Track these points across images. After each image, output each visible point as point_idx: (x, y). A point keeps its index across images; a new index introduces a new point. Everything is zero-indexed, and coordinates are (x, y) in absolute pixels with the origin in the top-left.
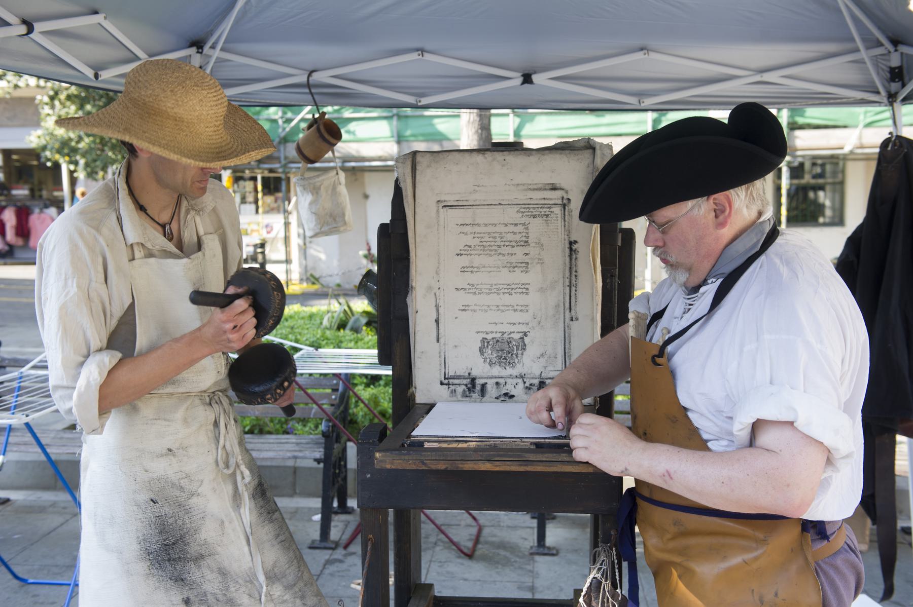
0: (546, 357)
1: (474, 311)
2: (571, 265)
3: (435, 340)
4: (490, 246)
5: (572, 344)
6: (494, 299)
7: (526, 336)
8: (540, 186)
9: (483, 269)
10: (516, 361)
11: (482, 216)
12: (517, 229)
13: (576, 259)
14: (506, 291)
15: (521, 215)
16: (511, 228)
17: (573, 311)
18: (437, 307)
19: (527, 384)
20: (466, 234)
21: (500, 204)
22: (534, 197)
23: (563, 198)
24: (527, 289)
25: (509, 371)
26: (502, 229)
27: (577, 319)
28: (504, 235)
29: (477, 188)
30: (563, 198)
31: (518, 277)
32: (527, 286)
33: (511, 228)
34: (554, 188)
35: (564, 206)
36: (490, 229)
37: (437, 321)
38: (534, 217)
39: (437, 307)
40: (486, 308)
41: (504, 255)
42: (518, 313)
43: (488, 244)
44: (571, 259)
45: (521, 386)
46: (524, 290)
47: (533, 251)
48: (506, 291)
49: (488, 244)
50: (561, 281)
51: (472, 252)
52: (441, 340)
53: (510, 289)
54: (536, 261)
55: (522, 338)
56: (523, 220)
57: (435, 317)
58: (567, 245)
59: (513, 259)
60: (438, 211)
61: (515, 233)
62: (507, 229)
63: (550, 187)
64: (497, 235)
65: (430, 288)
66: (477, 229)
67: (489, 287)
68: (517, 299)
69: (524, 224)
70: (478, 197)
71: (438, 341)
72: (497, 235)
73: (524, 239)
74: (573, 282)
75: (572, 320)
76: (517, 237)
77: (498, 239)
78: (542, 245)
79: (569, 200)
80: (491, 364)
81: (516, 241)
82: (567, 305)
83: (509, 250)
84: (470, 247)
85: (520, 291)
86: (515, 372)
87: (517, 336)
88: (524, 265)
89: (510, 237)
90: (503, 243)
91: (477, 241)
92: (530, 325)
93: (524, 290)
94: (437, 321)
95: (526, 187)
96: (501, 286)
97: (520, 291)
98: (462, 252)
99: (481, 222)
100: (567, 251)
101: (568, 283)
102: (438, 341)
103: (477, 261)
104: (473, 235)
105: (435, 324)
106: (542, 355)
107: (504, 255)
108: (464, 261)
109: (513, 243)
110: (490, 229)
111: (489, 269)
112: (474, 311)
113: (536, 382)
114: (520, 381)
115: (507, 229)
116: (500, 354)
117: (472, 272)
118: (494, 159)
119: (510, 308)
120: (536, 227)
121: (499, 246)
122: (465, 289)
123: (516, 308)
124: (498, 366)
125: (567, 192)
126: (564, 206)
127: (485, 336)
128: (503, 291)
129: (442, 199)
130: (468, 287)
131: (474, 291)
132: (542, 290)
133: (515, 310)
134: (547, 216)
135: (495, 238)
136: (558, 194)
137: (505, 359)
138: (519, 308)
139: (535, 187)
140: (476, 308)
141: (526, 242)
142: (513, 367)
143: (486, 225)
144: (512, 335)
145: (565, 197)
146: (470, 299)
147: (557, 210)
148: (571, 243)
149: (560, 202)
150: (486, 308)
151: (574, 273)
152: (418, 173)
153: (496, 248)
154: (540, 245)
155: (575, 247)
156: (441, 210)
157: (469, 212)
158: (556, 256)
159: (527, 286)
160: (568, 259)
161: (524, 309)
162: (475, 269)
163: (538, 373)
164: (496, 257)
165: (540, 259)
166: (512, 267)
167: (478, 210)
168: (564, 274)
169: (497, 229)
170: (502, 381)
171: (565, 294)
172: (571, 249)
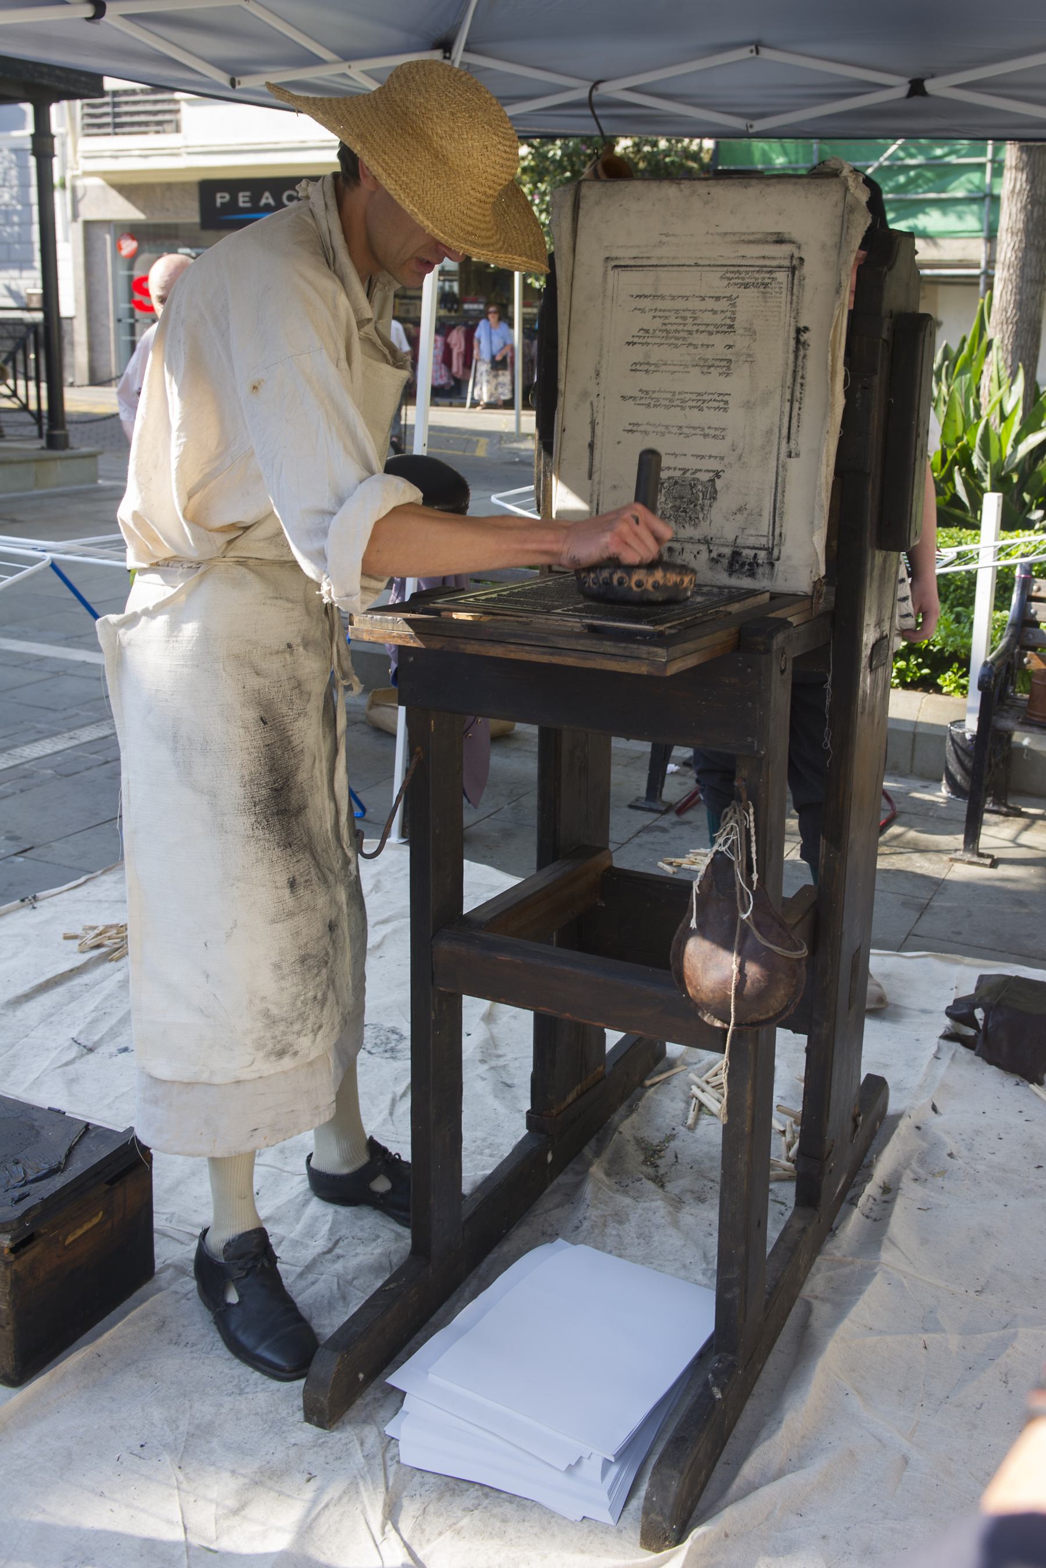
1: (646, 433)
2: (796, 366)
3: (586, 476)
4: (676, 331)
5: (786, 493)
7: (719, 477)
8: (758, 236)
9: (664, 368)
10: (701, 516)
11: (670, 282)
13: (805, 356)
14: (694, 404)
15: (726, 282)
16: (710, 304)
17: (792, 442)
18: (593, 423)
19: (714, 555)
20: (643, 311)
21: (697, 265)
22: (748, 254)
23: (792, 256)
24: (726, 402)
25: (688, 531)
26: (697, 304)
27: (797, 455)
28: (698, 314)
29: (664, 239)
30: (792, 256)
32: (726, 398)
33: (710, 304)
35: (793, 269)
36: (680, 304)
37: (591, 446)
38: (746, 286)
39: (593, 423)
40: (663, 429)
41: (695, 346)
42: (710, 440)
43: (674, 327)
44: (796, 357)
45: (704, 556)
46: (721, 405)
47: (740, 342)
49: (674, 327)
50: (779, 391)
51: (649, 340)
52: (596, 477)
53: (700, 401)
54: (743, 358)
55: (712, 481)
56: (729, 291)
57: (589, 439)
58: (793, 335)
59: (709, 354)
60: (605, 274)
61: (715, 312)
62: (703, 305)
63: (775, 238)
64: (688, 314)
65: (585, 394)
66: (659, 304)
67: (669, 396)
68: (710, 418)
69: (730, 298)
71: (590, 477)
72: (688, 314)
73: (728, 322)
74: (797, 394)
75: (790, 456)
76: (718, 319)
77: (689, 321)
78: (755, 333)
79: (801, 259)
82: (785, 431)
83: (703, 338)
84: (647, 331)
85: (716, 404)
86: (696, 533)
87: (704, 477)
88: (724, 363)
89: (708, 318)
90: (695, 328)
91: (658, 323)
92: (726, 461)
93: (721, 405)
94: (591, 446)
96: (688, 396)
97: (716, 404)
98: (636, 340)
99: (666, 293)
100: (792, 343)
101: (788, 397)
102: (590, 477)
103: (657, 354)
104: (652, 313)
106: (740, 510)
107: (695, 346)
108: (637, 354)
109: (711, 328)
110: (680, 304)
111: (673, 368)
113: (727, 551)
114: (703, 548)
116: (678, 503)
119: (698, 431)
120: (748, 301)
121: (690, 332)
122: (635, 398)
123: (707, 431)
124: (673, 523)
125: (799, 247)
126: (793, 269)
128: (690, 403)
129: (614, 255)
130: (640, 394)
133: (705, 436)
134: (766, 285)
135: (684, 318)
136: (786, 249)
137: (685, 511)
138: (712, 432)
139: (752, 238)
140: (650, 429)
141: (731, 326)
142: (696, 526)
143: (673, 298)
144: (698, 475)
145: (796, 255)
147: (782, 277)
148: (799, 331)
149: (787, 263)
150: (663, 429)
151: (799, 380)
152: (581, 213)
153: (685, 335)
154: (751, 332)
155: (804, 337)
156: (610, 273)
157: (650, 275)
158: (775, 353)
159: (726, 398)
160: (791, 356)
162: (652, 368)
163: (731, 538)
164: (683, 350)
165: (749, 355)
166: (706, 366)
167: (663, 274)
168: (784, 381)
170: (677, 546)
171: (782, 413)
172: (798, 341)
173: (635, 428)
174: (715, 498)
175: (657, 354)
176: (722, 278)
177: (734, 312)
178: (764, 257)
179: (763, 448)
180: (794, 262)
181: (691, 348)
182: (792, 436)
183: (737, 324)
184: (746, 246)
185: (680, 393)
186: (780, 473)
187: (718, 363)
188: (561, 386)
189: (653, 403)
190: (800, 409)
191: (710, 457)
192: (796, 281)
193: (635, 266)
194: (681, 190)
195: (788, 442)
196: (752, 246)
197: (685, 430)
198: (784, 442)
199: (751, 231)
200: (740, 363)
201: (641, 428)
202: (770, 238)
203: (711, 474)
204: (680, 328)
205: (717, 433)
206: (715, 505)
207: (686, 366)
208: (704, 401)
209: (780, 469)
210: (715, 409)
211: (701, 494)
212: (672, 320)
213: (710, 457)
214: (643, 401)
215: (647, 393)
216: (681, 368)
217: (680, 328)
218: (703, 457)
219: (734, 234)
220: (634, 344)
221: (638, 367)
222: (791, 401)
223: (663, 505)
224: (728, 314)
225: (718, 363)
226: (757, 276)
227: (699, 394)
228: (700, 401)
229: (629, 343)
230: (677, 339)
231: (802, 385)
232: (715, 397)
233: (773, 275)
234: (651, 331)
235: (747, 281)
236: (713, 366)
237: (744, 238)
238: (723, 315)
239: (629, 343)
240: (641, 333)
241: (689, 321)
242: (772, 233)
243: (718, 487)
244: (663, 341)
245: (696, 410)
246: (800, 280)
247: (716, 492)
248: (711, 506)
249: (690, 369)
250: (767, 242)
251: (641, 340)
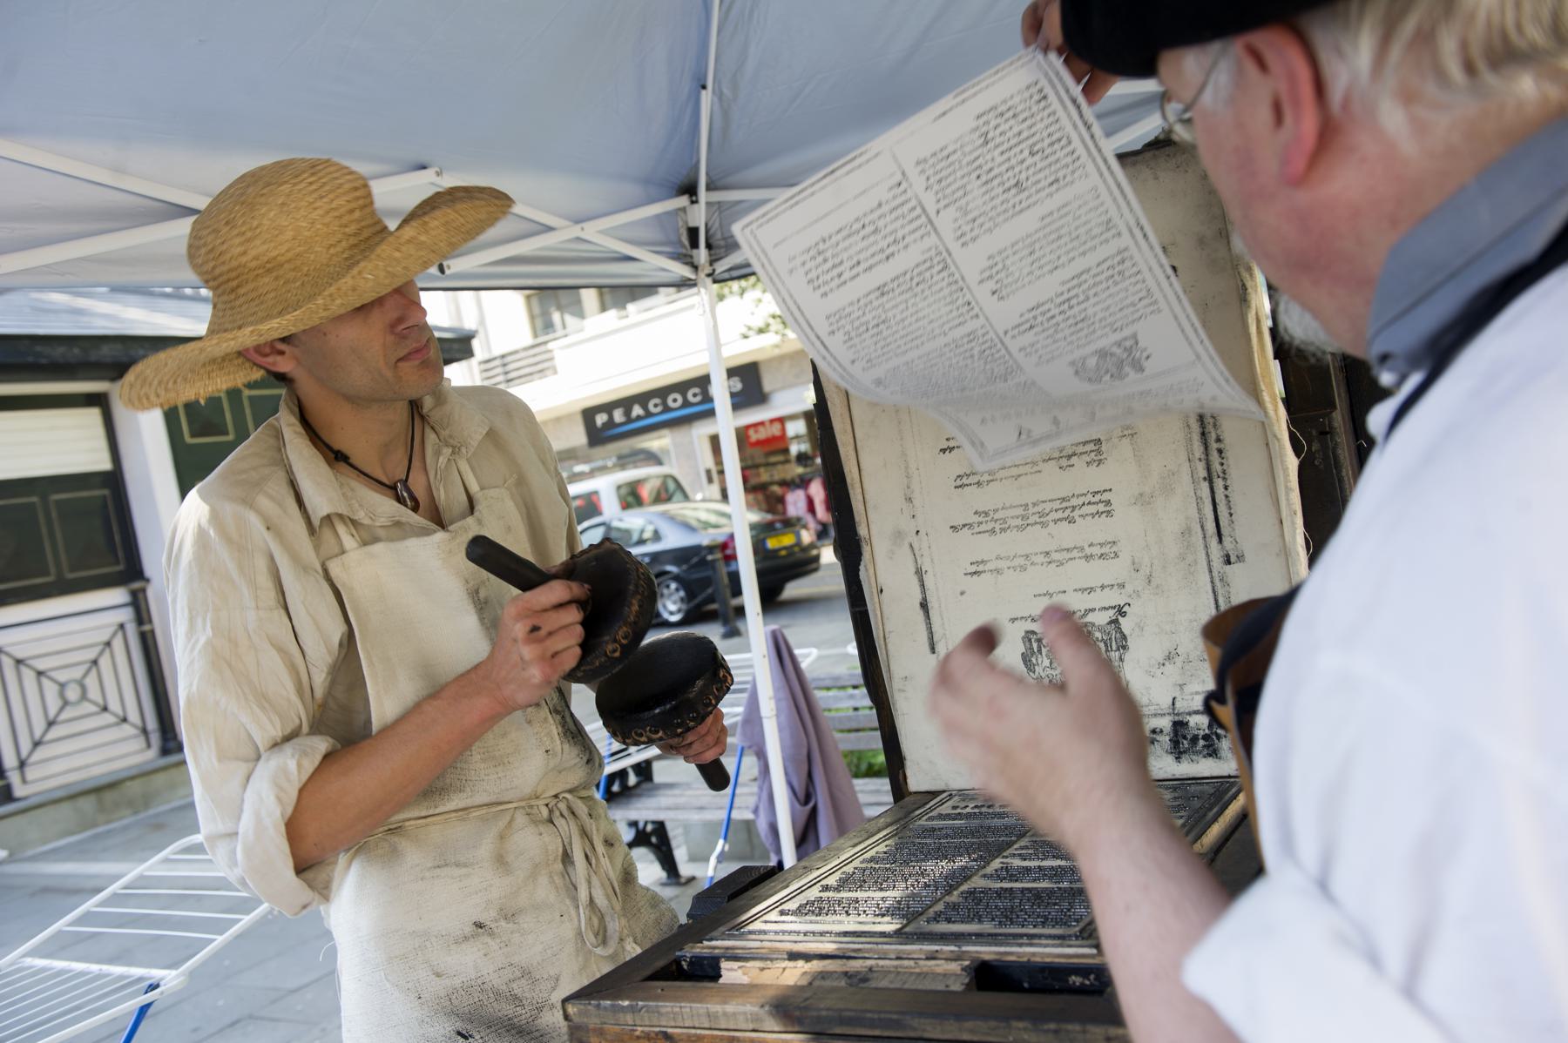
0: (1179, 660)
1: (998, 571)
6: (1035, 540)
7: (1123, 614)
14: (1060, 515)
17: (1227, 540)
24: (1108, 503)
27: (1240, 558)
31: (1084, 478)
32: (1105, 496)
40: (1021, 561)
42: (1096, 563)
46: (1101, 507)
48: (1060, 515)
50: (1186, 469)
53: (1068, 511)
55: (1115, 622)
65: (898, 535)
67: (1020, 511)
68: (1089, 530)
71: (933, 650)
74: (1216, 467)
75: (1228, 562)
85: (1093, 509)
87: (1101, 619)
92: (1129, 588)
93: (1101, 507)
94: (924, 606)
96: (1048, 507)
101: (1203, 473)
102: (933, 650)
106: (1169, 658)
111: (1015, 471)
112: (998, 571)
119: (1075, 553)
123: (1088, 551)
130: (976, 519)
131: (990, 526)
132: (1142, 500)
133: (1088, 558)
138: (1097, 550)
140: (1002, 564)
144: (1090, 618)
146: (986, 547)
150: (1021, 561)
151: (1214, 446)
159: (1105, 496)
161: (1108, 551)
166: (1066, 458)
168: (1190, 452)
171: (1199, 499)
173: (981, 568)
174: (1124, 647)
182: (1224, 531)
185: (1034, 505)
186: (1220, 591)
187: (1081, 449)
188: (862, 531)
189: (998, 527)
190: (1226, 488)
191: (1103, 587)
195: (1220, 541)
197: (1055, 556)
198: (1214, 542)
200: (1115, 440)
201: (990, 566)
203: (1111, 613)
205: (1105, 550)
206: (1127, 657)
207: (1034, 463)
208: (1074, 508)
209: (1218, 584)
210: (1093, 515)
211: (1102, 645)
213: (1103, 587)
214: (983, 527)
215: (986, 514)
216: (1028, 469)
218: (1091, 590)
221: (965, 481)
222: (1210, 479)
223: (1049, 671)
225: (1081, 449)
227: (1064, 499)
231: (1220, 451)
232: (1090, 498)
236: (1074, 454)
239: (943, 451)
243: (1126, 630)
245: (1065, 523)
247: (1124, 637)
248: (1121, 659)
249: (1041, 466)
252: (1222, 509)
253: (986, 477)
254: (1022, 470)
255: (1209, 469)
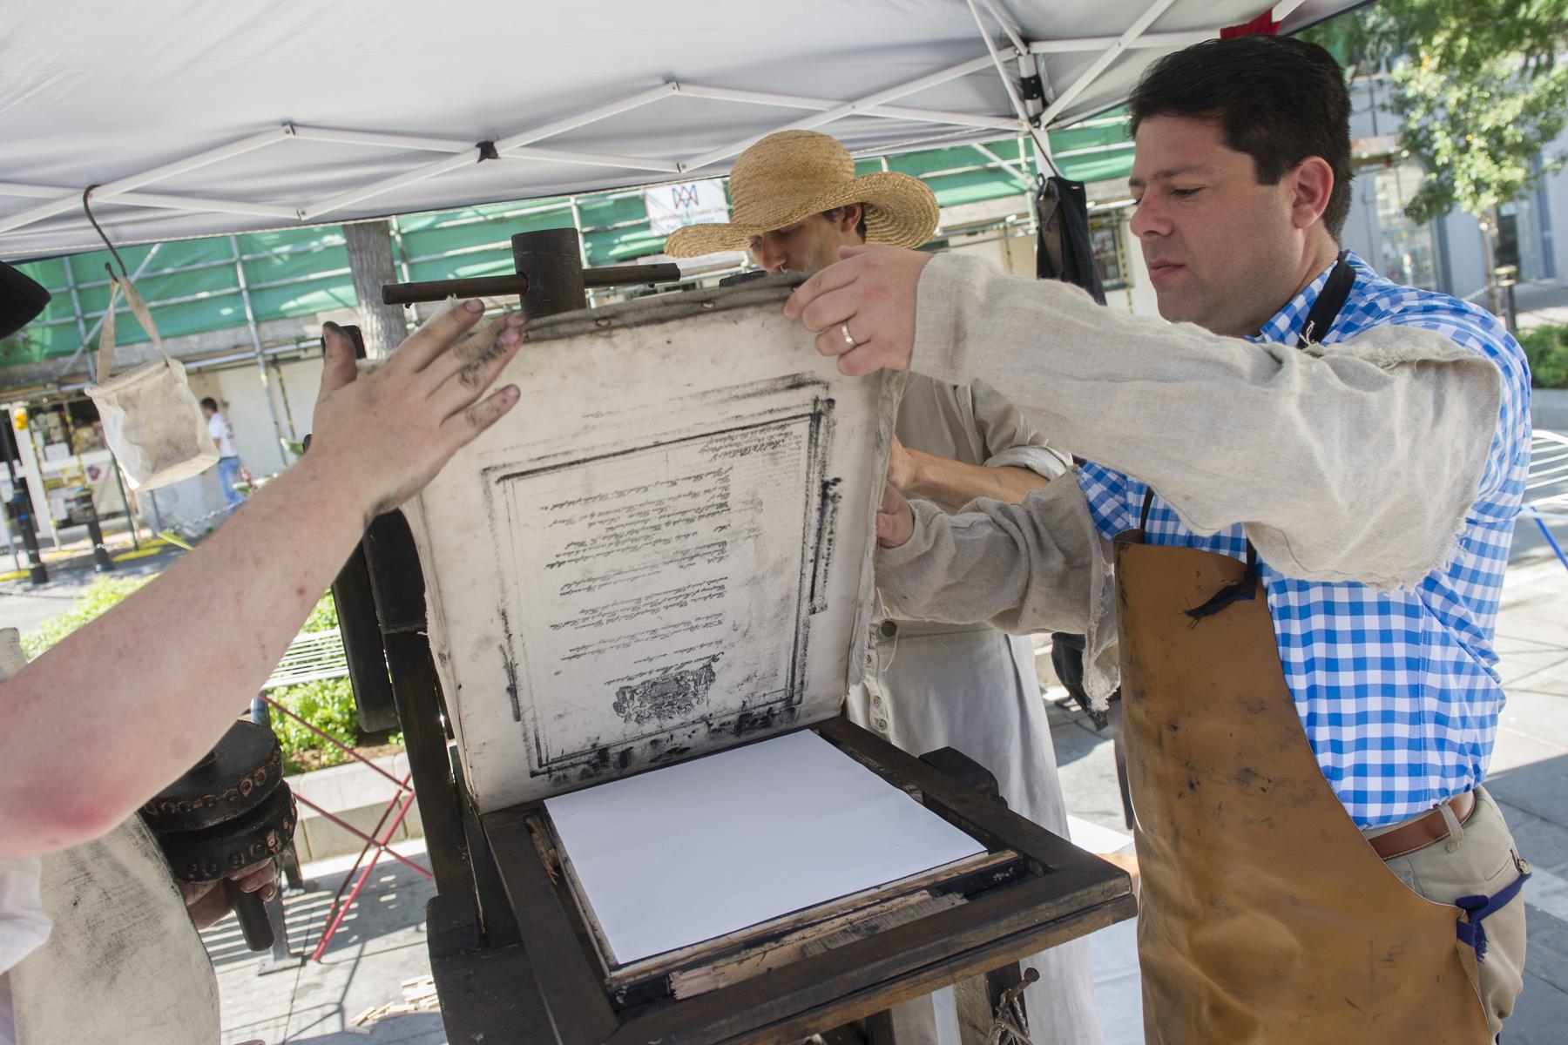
2: (821, 521)
9: (618, 578)
10: (694, 701)
11: (607, 476)
12: (699, 486)
13: (835, 510)
15: (711, 454)
18: (511, 670)
20: (569, 522)
21: (657, 445)
24: (722, 587)
26: (665, 492)
29: (592, 421)
30: (816, 401)
31: (704, 571)
34: (797, 384)
35: (816, 417)
37: (512, 690)
39: (511, 670)
41: (667, 541)
43: (628, 528)
46: (715, 591)
52: (527, 716)
55: (708, 667)
58: (816, 489)
59: (690, 544)
60: (487, 492)
61: (695, 495)
62: (674, 491)
63: (788, 382)
65: (486, 641)
66: (597, 507)
67: (633, 604)
69: (719, 472)
70: (601, 441)
73: (719, 501)
74: (824, 551)
76: (701, 501)
77: (653, 515)
78: (761, 503)
79: (831, 402)
80: (640, 719)
81: (699, 510)
83: (682, 529)
84: (582, 544)
85: (706, 593)
86: (692, 716)
89: (683, 504)
91: (600, 530)
93: (715, 591)
95: (725, 395)
97: (706, 593)
98: (561, 559)
100: (816, 501)
101: (810, 555)
104: (588, 520)
105: (507, 698)
107: (667, 541)
109: (689, 515)
110: (635, 499)
111: (633, 574)
115: (674, 491)
117: (589, 588)
118: (639, 345)
120: (747, 473)
121: (657, 528)
122: (575, 622)
126: (816, 417)
127: (626, 683)
128: (667, 603)
129: (498, 462)
134: (775, 445)
136: (807, 394)
139: (750, 390)
140: (602, 646)
141: (721, 505)
143: (621, 494)
144: (686, 668)
146: (589, 636)
147: (802, 429)
148: (825, 485)
149: (809, 410)
151: (826, 536)
154: (755, 504)
156: (497, 490)
160: (815, 515)
162: (599, 582)
169: (652, 495)
172: (824, 496)
175: (600, 567)
176: (703, 451)
177: (725, 488)
178: (771, 411)
179: (777, 615)
180: (819, 407)
181: (661, 546)
183: (730, 501)
184: (740, 402)
189: (604, 620)
192: (822, 429)
193: (544, 469)
194: (615, 346)
196: (751, 400)
197: (661, 632)
199: (749, 380)
202: (780, 385)
204: (639, 526)
212: (625, 520)
216: (646, 571)
217: (639, 526)
219: (719, 391)
220: (560, 564)
221: (574, 588)
222: (816, 562)
224: (718, 492)
226: (759, 436)
228: (681, 597)
229: (552, 566)
230: (633, 540)
233: (788, 430)
234: (589, 542)
235: (744, 446)
237: (735, 393)
238: (708, 496)
240: (571, 549)
241: (653, 515)
242: (783, 378)
244: (613, 548)
246: (828, 427)
249: (661, 567)
250: (775, 391)
251: (573, 557)
252: (820, 580)
253: (599, 582)
254: (640, 573)
255: (817, 554)
